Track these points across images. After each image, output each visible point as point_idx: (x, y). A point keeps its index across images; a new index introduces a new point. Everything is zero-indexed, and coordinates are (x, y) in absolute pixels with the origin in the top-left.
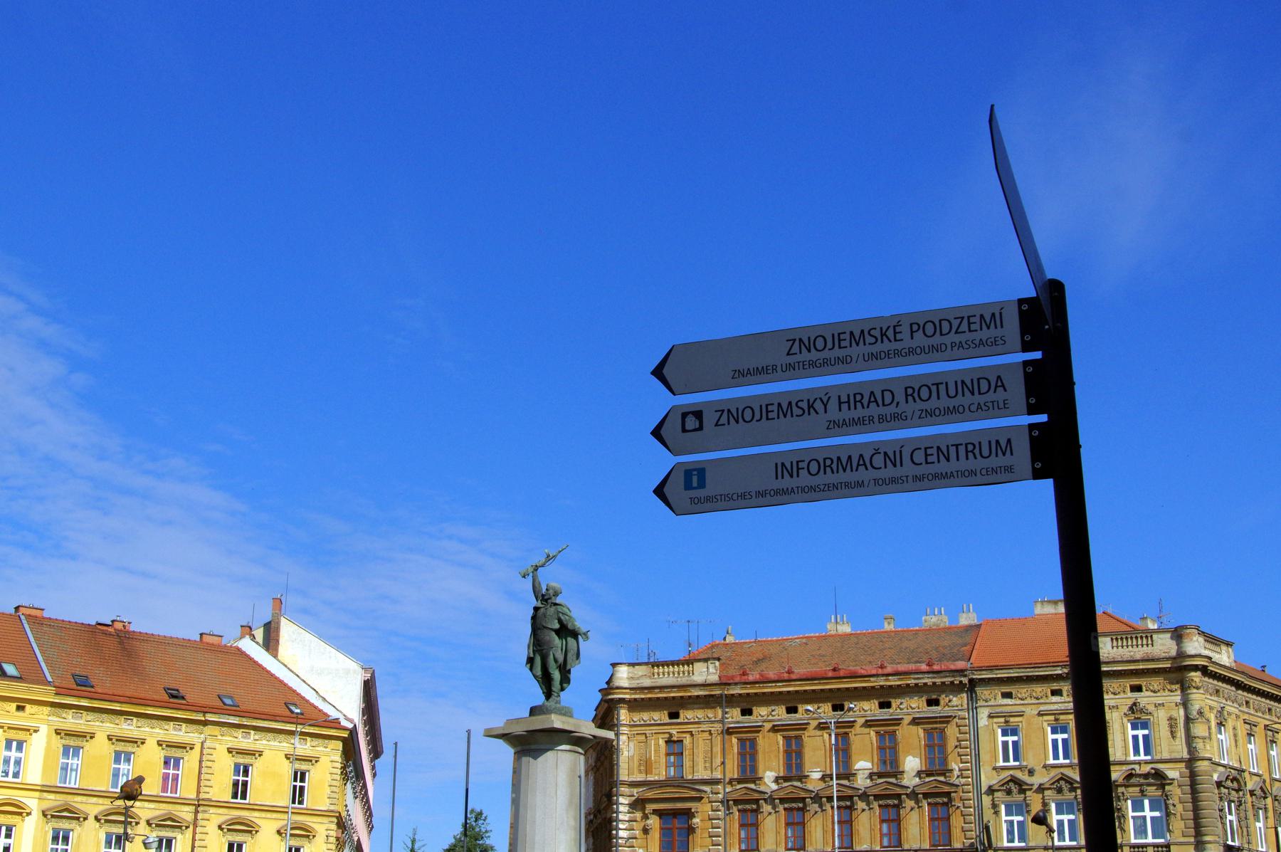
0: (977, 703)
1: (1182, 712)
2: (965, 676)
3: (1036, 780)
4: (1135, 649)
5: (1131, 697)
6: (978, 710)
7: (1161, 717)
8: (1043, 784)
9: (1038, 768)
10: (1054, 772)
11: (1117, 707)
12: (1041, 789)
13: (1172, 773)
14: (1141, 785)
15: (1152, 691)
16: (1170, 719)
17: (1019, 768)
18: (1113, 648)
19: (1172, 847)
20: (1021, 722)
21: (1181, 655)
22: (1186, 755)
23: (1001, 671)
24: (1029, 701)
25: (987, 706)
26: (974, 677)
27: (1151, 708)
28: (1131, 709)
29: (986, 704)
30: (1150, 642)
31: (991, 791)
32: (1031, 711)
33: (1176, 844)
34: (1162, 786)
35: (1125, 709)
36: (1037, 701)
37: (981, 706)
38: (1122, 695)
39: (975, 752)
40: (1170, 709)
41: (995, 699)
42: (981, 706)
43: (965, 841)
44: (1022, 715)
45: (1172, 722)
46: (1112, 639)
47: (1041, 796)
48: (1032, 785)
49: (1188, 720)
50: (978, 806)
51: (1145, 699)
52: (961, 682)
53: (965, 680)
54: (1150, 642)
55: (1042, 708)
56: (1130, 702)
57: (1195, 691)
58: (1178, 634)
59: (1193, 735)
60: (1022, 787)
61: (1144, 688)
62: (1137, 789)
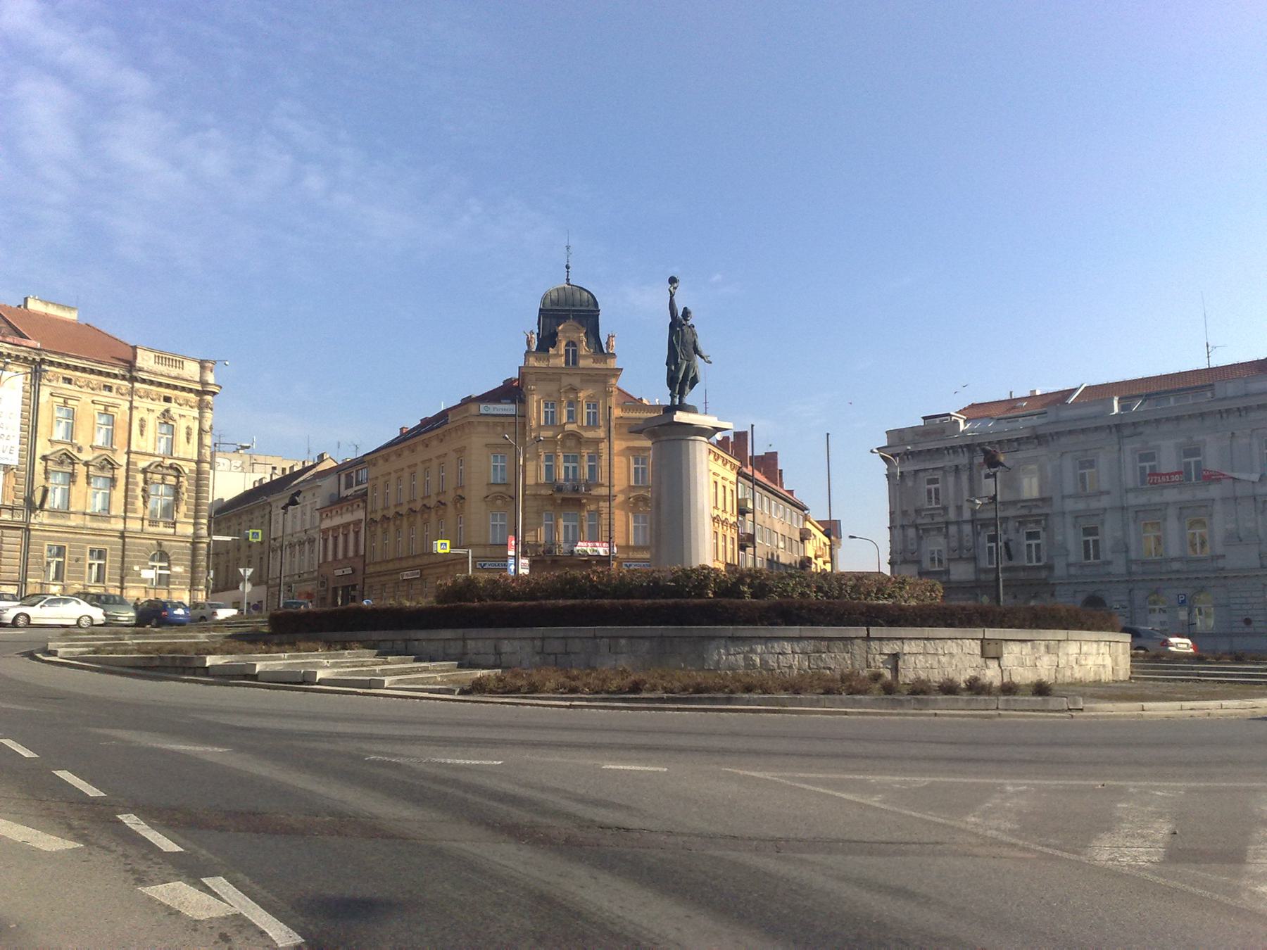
0: (40, 381)
1: (197, 423)
2: (39, 355)
3: (85, 456)
4: (170, 368)
5: (161, 406)
6: (41, 388)
7: (181, 426)
8: (89, 461)
9: (87, 448)
10: (97, 453)
11: (153, 411)
12: (87, 464)
13: (188, 467)
14: (163, 475)
15: (178, 404)
16: (188, 428)
17: (72, 445)
18: (155, 362)
19: (177, 525)
20: (77, 406)
21: (203, 383)
22: (195, 458)
23: (100, 365)
24: (85, 390)
25: (50, 386)
26: (47, 358)
27: (176, 417)
28: (163, 415)
29: (49, 384)
30: (181, 366)
31: (44, 458)
32: (87, 399)
33: (180, 522)
34: (177, 477)
35: (158, 414)
36: (92, 392)
37: (44, 385)
38: (157, 402)
39: (33, 423)
40: (189, 420)
41: (58, 381)
42: (44, 385)
43: (15, 500)
44: (78, 400)
45: (189, 429)
46: (155, 356)
47: (86, 468)
48: (82, 460)
49: (201, 431)
50: (30, 470)
51: (175, 409)
52: (34, 359)
53: (38, 359)
54: (181, 366)
55: (95, 398)
56: (162, 409)
57: (210, 411)
58: (203, 365)
59: (204, 443)
60: (72, 461)
61: (173, 401)
62: (160, 476)
